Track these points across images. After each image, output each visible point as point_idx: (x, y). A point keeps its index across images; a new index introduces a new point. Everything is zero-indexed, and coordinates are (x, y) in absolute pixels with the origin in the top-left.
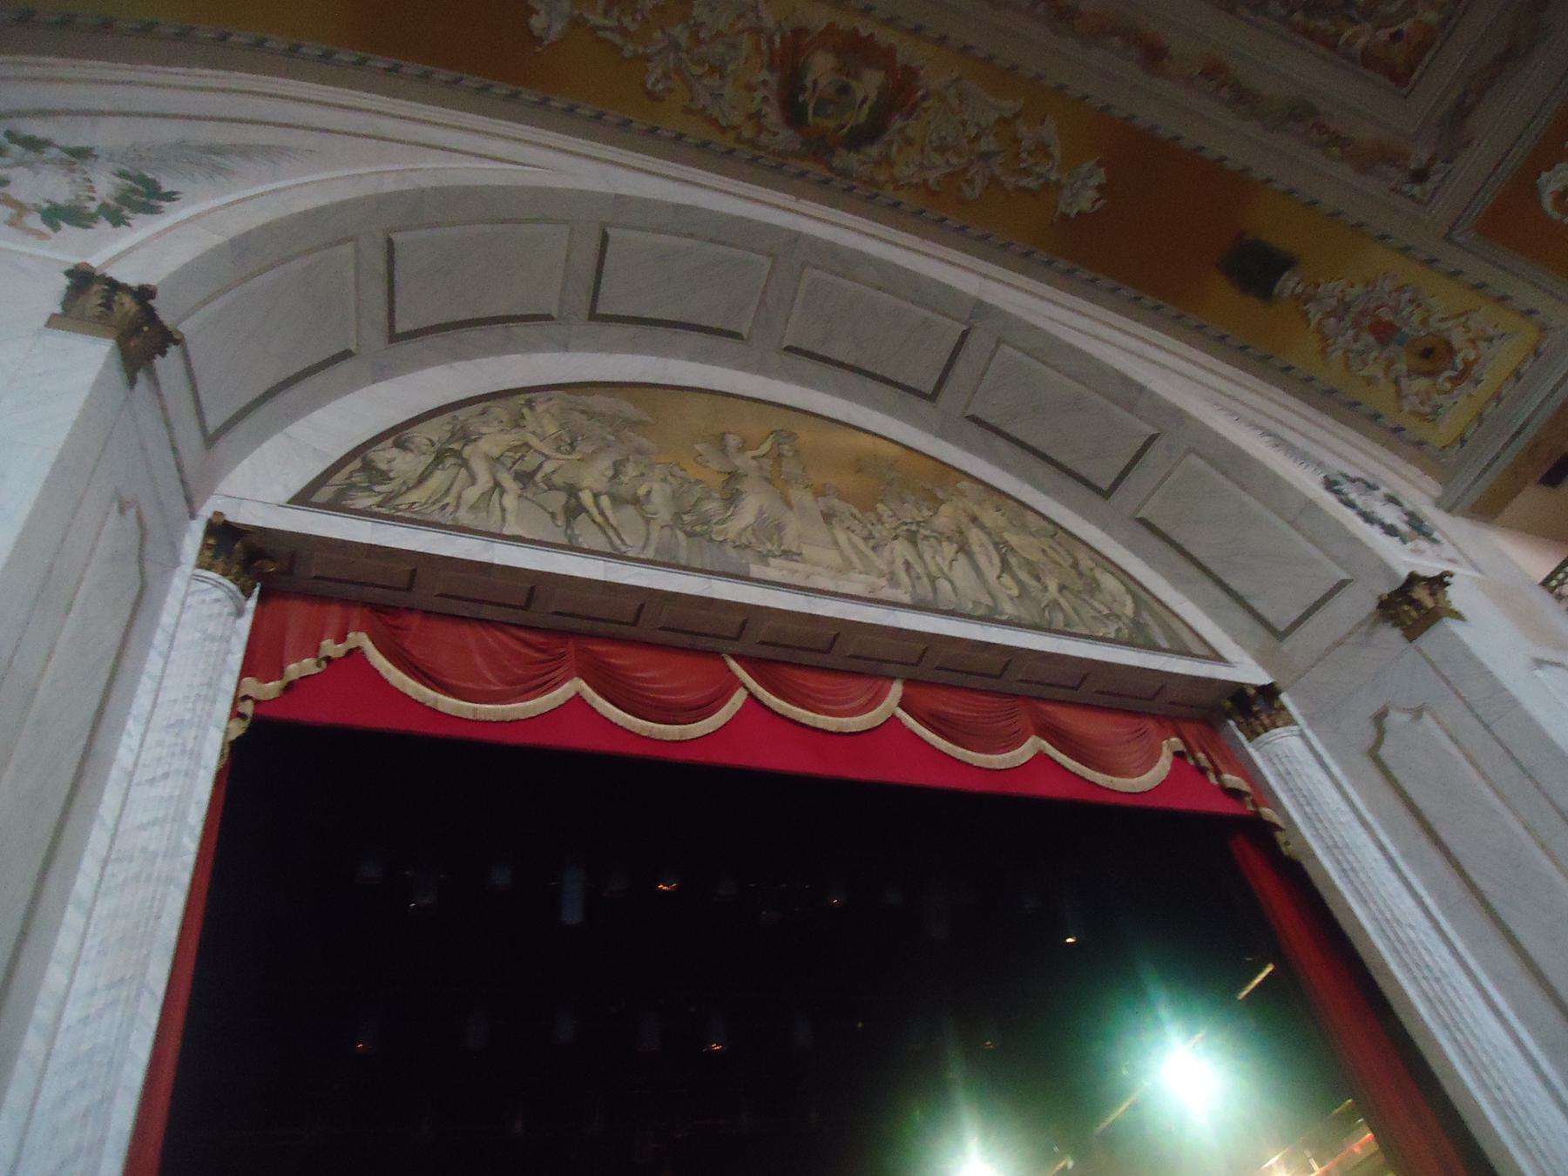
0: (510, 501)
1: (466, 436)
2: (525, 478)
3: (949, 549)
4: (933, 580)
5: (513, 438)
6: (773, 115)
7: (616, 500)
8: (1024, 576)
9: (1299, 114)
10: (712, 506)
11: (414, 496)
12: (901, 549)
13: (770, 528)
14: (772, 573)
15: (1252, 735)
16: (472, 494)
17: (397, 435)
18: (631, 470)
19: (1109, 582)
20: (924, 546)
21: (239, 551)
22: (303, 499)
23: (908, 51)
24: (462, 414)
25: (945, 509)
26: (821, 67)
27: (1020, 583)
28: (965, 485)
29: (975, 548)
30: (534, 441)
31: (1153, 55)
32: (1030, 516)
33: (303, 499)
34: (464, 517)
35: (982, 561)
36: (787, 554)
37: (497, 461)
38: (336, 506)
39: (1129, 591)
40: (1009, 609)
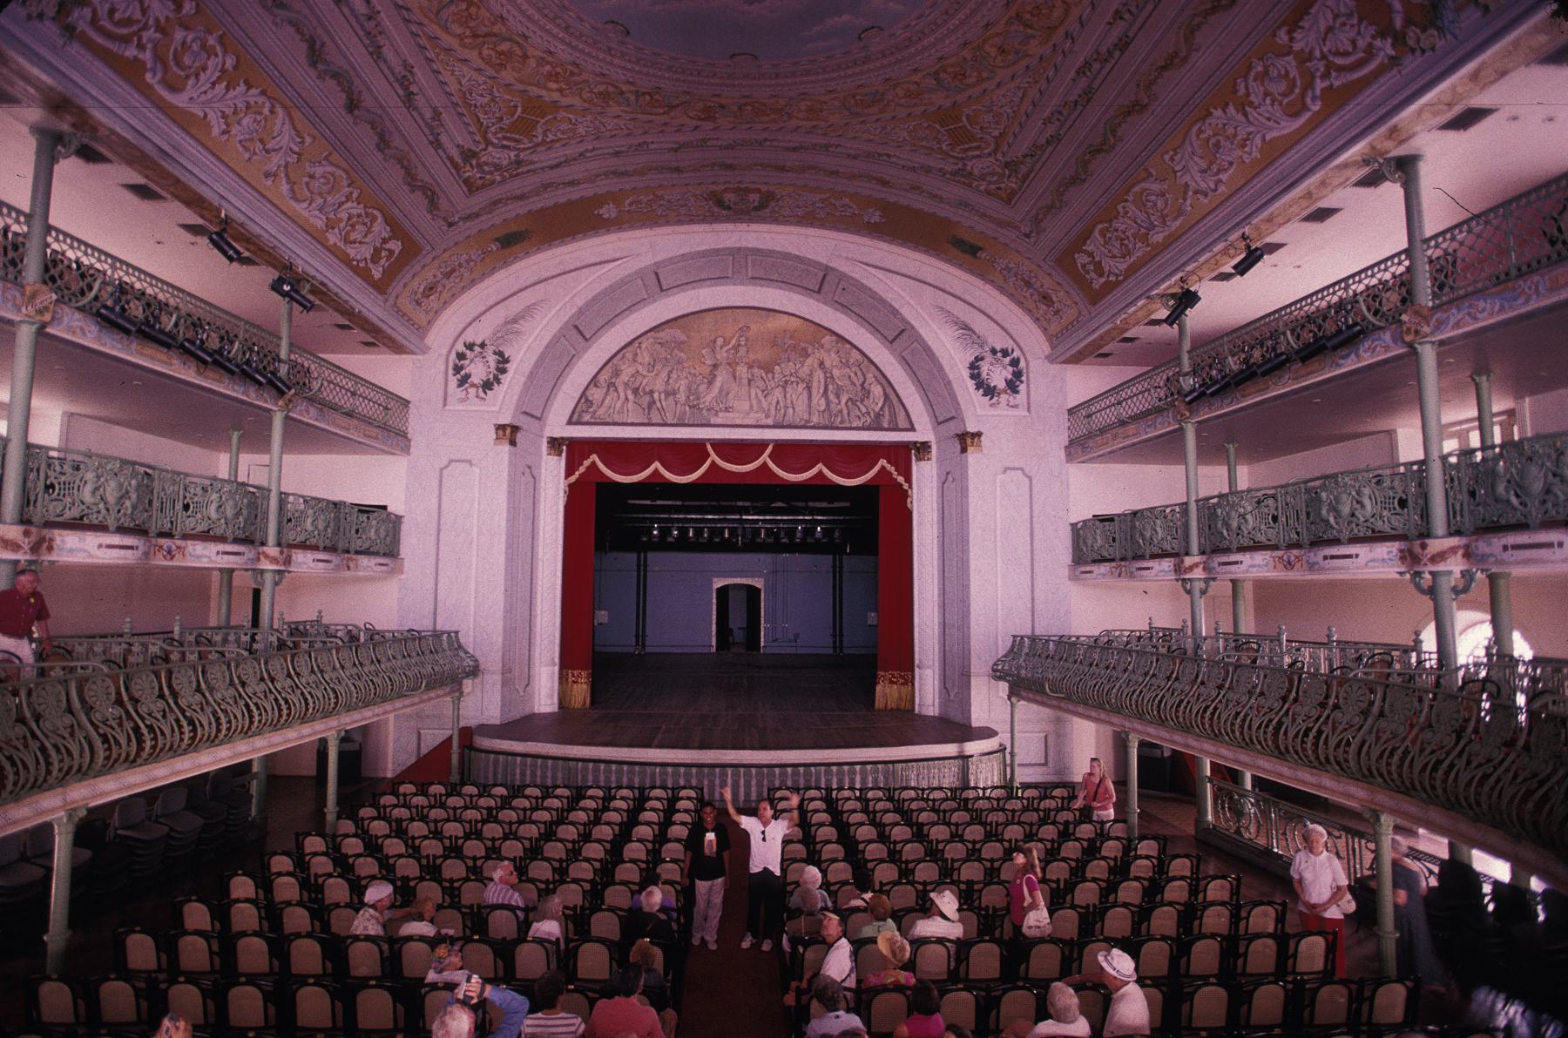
0: (630, 405)
1: (617, 373)
2: (636, 391)
3: (801, 386)
4: (786, 407)
5: (632, 370)
6: (716, 210)
7: (668, 394)
8: (832, 397)
9: (963, 204)
10: (703, 388)
11: (601, 411)
12: (778, 393)
13: (724, 393)
14: (719, 421)
15: (918, 459)
16: (619, 404)
17: (594, 381)
18: (674, 376)
19: (877, 390)
20: (789, 389)
21: (555, 444)
22: (570, 422)
23: (764, 188)
24: (615, 361)
25: (809, 361)
26: (729, 197)
27: (828, 403)
28: (828, 339)
29: (815, 384)
30: (640, 368)
31: (884, 183)
32: (854, 353)
33: (570, 422)
34: (617, 418)
35: (814, 392)
36: (727, 410)
37: (626, 384)
38: (579, 423)
39: (886, 396)
40: (815, 419)
